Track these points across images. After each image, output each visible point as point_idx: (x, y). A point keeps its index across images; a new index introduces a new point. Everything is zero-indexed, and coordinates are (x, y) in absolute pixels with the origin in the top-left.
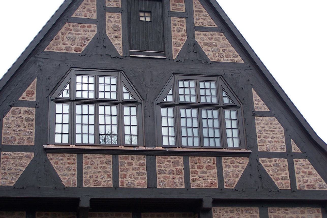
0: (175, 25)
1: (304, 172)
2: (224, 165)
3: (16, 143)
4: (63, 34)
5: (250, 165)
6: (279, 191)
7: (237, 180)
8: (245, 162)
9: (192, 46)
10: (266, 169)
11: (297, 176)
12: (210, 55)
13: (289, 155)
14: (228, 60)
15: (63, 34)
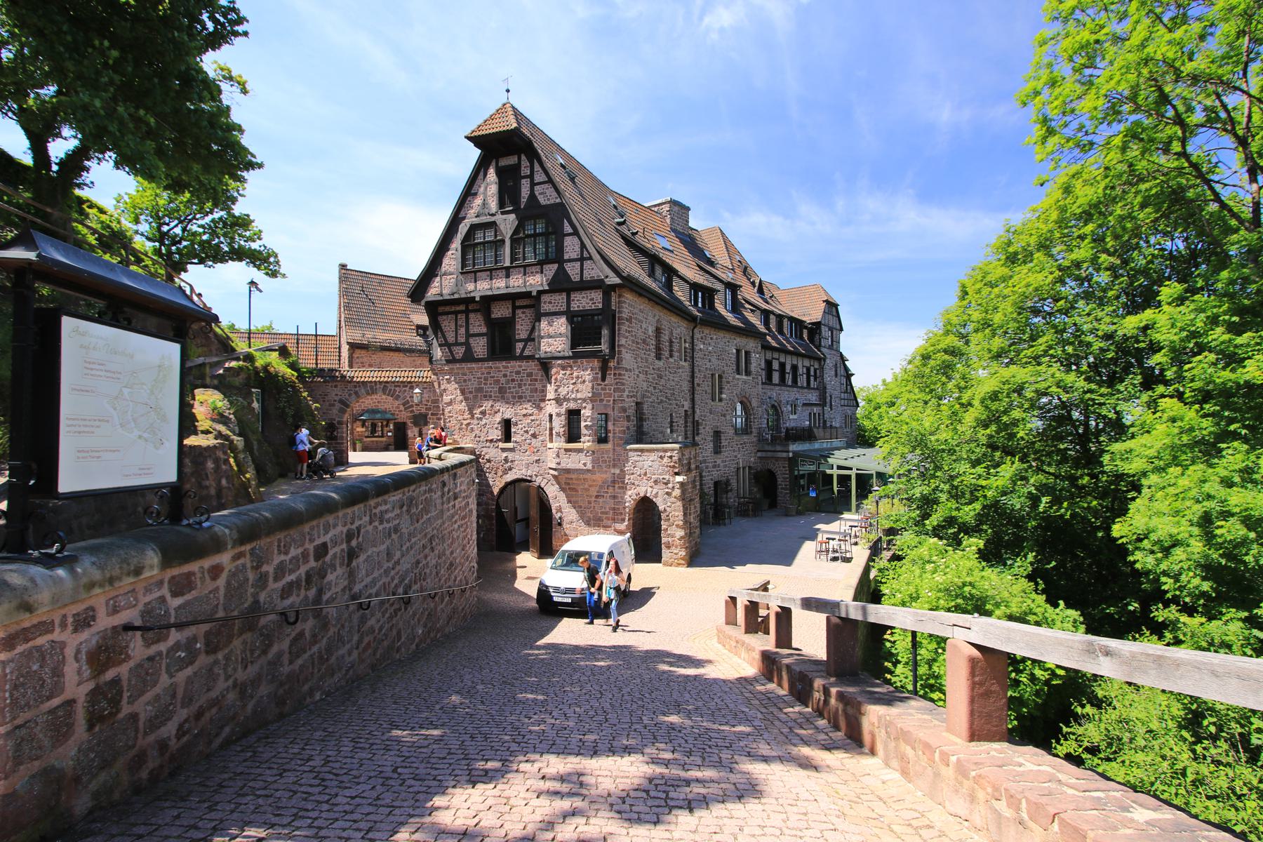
8: (556, 266)
9: (532, 196)
12: (542, 200)
14: (552, 202)
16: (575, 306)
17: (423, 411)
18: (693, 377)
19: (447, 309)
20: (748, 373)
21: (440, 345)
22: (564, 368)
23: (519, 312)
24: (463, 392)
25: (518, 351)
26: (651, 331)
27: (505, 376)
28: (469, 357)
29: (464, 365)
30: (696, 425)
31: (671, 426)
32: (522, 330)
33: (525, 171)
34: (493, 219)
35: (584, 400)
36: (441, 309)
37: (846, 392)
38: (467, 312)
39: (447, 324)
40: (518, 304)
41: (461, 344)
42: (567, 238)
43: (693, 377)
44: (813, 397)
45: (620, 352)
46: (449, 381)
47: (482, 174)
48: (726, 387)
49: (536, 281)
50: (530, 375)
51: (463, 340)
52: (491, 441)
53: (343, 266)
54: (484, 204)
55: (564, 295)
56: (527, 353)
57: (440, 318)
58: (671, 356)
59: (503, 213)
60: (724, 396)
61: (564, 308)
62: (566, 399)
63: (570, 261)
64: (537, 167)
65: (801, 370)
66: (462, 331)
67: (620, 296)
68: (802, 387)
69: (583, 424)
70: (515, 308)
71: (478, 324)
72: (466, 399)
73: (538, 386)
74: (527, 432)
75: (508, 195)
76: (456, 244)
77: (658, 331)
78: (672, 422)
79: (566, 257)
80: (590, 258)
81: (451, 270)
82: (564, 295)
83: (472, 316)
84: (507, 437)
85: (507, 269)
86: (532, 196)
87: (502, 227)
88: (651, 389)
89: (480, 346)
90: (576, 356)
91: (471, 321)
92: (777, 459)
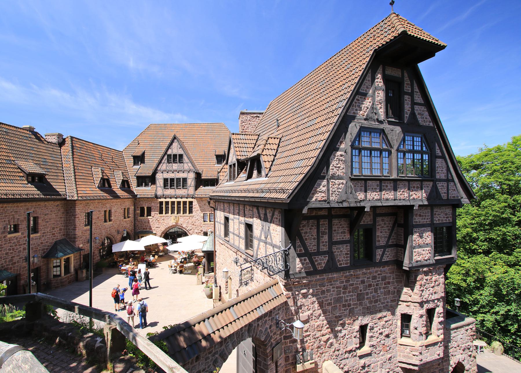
0: (406, 100)
4: (355, 103)
5: (433, 186)
6: (443, 199)
9: (413, 114)
11: (450, 191)
15: (355, 103)
16: (436, 220)
17: (278, 337)
21: (299, 256)
22: (426, 274)
24: (321, 305)
27: (363, 282)
28: (332, 267)
29: (325, 276)
33: (407, 88)
35: (438, 300)
39: (309, 233)
41: (324, 253)
46: (305, 296)
49: (418, 197)
50: (384, 279)
52: (350, 351)
56: (385, 259)
62: (428, 302)
64: (416, 89)
66: (326, 238)
72: (324, 312)
74: (381, 334)
76: (345, 145)
80: (453, 181)
81: (340, 173)
83: (335, 221)
85: (395, 180)
86: (413, 114)
89: (343, 254)
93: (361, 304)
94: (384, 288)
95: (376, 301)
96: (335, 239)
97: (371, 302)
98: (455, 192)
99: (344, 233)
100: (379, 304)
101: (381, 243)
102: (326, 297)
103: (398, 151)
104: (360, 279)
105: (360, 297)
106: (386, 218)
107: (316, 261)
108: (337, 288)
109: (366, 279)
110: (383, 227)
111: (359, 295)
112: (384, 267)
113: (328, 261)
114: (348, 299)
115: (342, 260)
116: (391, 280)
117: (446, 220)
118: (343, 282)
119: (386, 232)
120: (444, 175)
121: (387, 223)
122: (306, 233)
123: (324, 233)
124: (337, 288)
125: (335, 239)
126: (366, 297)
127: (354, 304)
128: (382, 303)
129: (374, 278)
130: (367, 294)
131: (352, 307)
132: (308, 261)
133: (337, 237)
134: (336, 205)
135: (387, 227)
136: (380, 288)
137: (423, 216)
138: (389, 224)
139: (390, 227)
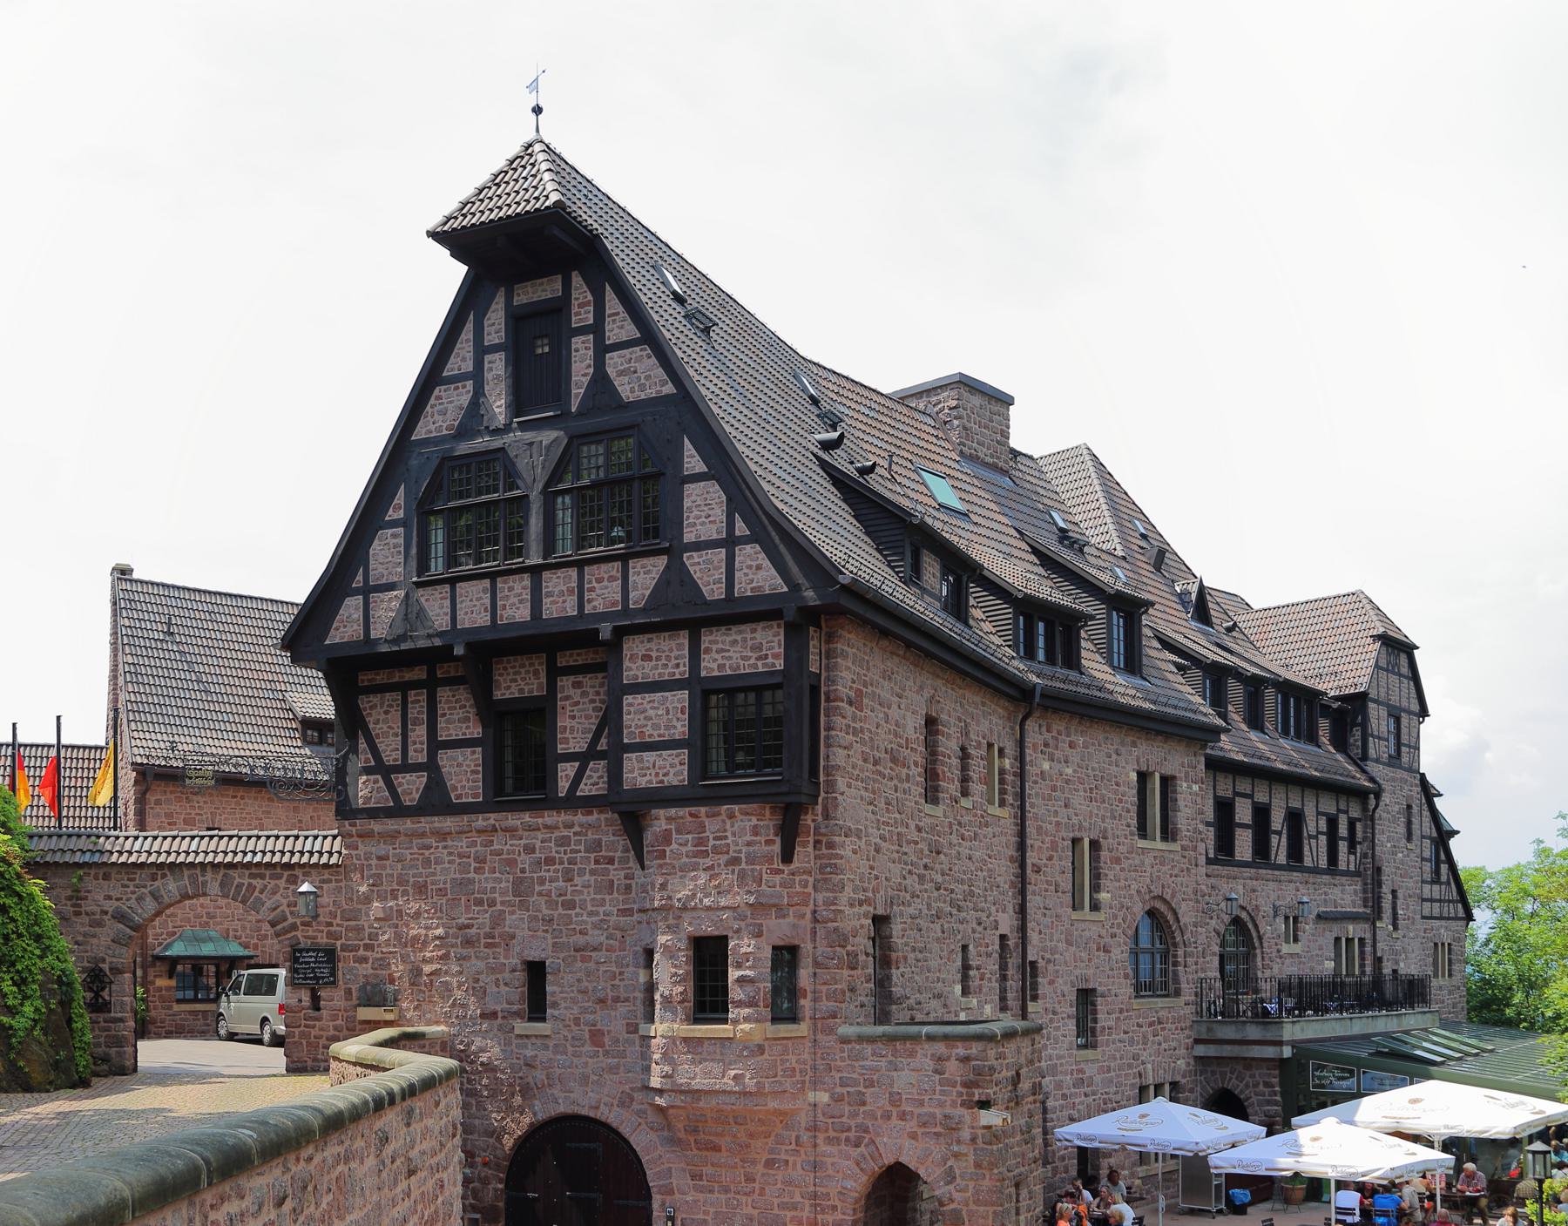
1: (750, 567)
2: (631, 571)
3: (384, 581)
6: (707, 603)
7: (648, 593)
8: (661, 562)
10: (692, 570)
13: (730, 543)
16: (711, 666)
18: (1022, 847)
19: (381, 678)
20: (1168, 833)
23: (565, 682)
25: (563, 786)
26: (913, 727)
27: (530, 849)
28: (437, 801)
30: (1030, 971)
31: (965, 978)
32: (574, 727)
34: (497, 443)
36: (365, 678)
37: (1436, 880)
38: (431, 686)
39: (382, 718)
40: (562, 661)
41: (416, 768)
42: (689, 489)
43: (1022, 847)
44: (1346, 895)
45: (831, 785)
47: (468, 333)
48: (1109, 871)
51: (422, 758)
53: (122, 573)
54: (475, 408)
55: (684, 639)
56: (585, 789)
57: (364, 702)
58: (965, 793)
59: (524, 426)
60: (1104, 896)
61: (683, 671)
63: (698, 546)
65: (1314, 824)
66: (419, 733)
67: (830, 638)
68: (1315, 871)
69: (733, 974)
70: (554, 673)
71: (459, 718)
73: (616, 875)
75: (536, 386)
77: (931, 723)
78: (966, 967)
79: (689, 537)
82: (684, 639)
83: (443, 694)
84: (537, 1006)
87: (522, 464)
88: (911, 881)
89: (464, 773)
90: (715, 797)
91: (442, 707)
92: (1249, 1063)
93: (524, 905)
94: (593, 872)
95: (570, 905)
96: (443, 736)
97: (552, 905)
98: (762, 573)
99: (467, 719)
100: (577, 915)
101: (571, 744)
102: (434, 874)
103: (549, 497)
104: (522, 842)
105: (520, 888)
106: (586, 679)
107: (401, 784)
108: (460, 856)
109: (538, 845)
110: (577, 703)
111: (518, 883)
112: (590, 813)
113: (427, 787)
114: (489, 886)
115: (463, 787)
116: (619, 854)
117: (755, 666)
118: (474, 844)
119: (587, 717)
120: (714, 527)
121: (591, 691)
122: (377, 722)
123: (416, 722)
124: (460, 856)
125: (443, 736)
126: (537, 888)
127: (503, 903)
128: (591, 914)
129: (563, 842)
130: (542, 881)
131: (499, 907)
132: (381, 783)
133: (447, 731)
134: (384, 648)
135: (593, 701)
136: (581, 873)
137: (658, 659)
138: (598, 693)
139: (602, 701)
